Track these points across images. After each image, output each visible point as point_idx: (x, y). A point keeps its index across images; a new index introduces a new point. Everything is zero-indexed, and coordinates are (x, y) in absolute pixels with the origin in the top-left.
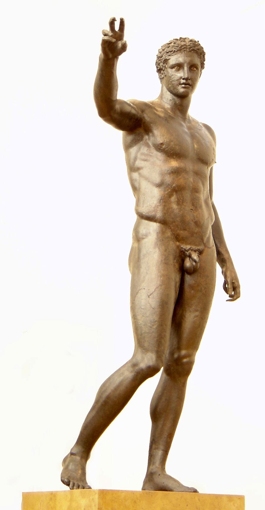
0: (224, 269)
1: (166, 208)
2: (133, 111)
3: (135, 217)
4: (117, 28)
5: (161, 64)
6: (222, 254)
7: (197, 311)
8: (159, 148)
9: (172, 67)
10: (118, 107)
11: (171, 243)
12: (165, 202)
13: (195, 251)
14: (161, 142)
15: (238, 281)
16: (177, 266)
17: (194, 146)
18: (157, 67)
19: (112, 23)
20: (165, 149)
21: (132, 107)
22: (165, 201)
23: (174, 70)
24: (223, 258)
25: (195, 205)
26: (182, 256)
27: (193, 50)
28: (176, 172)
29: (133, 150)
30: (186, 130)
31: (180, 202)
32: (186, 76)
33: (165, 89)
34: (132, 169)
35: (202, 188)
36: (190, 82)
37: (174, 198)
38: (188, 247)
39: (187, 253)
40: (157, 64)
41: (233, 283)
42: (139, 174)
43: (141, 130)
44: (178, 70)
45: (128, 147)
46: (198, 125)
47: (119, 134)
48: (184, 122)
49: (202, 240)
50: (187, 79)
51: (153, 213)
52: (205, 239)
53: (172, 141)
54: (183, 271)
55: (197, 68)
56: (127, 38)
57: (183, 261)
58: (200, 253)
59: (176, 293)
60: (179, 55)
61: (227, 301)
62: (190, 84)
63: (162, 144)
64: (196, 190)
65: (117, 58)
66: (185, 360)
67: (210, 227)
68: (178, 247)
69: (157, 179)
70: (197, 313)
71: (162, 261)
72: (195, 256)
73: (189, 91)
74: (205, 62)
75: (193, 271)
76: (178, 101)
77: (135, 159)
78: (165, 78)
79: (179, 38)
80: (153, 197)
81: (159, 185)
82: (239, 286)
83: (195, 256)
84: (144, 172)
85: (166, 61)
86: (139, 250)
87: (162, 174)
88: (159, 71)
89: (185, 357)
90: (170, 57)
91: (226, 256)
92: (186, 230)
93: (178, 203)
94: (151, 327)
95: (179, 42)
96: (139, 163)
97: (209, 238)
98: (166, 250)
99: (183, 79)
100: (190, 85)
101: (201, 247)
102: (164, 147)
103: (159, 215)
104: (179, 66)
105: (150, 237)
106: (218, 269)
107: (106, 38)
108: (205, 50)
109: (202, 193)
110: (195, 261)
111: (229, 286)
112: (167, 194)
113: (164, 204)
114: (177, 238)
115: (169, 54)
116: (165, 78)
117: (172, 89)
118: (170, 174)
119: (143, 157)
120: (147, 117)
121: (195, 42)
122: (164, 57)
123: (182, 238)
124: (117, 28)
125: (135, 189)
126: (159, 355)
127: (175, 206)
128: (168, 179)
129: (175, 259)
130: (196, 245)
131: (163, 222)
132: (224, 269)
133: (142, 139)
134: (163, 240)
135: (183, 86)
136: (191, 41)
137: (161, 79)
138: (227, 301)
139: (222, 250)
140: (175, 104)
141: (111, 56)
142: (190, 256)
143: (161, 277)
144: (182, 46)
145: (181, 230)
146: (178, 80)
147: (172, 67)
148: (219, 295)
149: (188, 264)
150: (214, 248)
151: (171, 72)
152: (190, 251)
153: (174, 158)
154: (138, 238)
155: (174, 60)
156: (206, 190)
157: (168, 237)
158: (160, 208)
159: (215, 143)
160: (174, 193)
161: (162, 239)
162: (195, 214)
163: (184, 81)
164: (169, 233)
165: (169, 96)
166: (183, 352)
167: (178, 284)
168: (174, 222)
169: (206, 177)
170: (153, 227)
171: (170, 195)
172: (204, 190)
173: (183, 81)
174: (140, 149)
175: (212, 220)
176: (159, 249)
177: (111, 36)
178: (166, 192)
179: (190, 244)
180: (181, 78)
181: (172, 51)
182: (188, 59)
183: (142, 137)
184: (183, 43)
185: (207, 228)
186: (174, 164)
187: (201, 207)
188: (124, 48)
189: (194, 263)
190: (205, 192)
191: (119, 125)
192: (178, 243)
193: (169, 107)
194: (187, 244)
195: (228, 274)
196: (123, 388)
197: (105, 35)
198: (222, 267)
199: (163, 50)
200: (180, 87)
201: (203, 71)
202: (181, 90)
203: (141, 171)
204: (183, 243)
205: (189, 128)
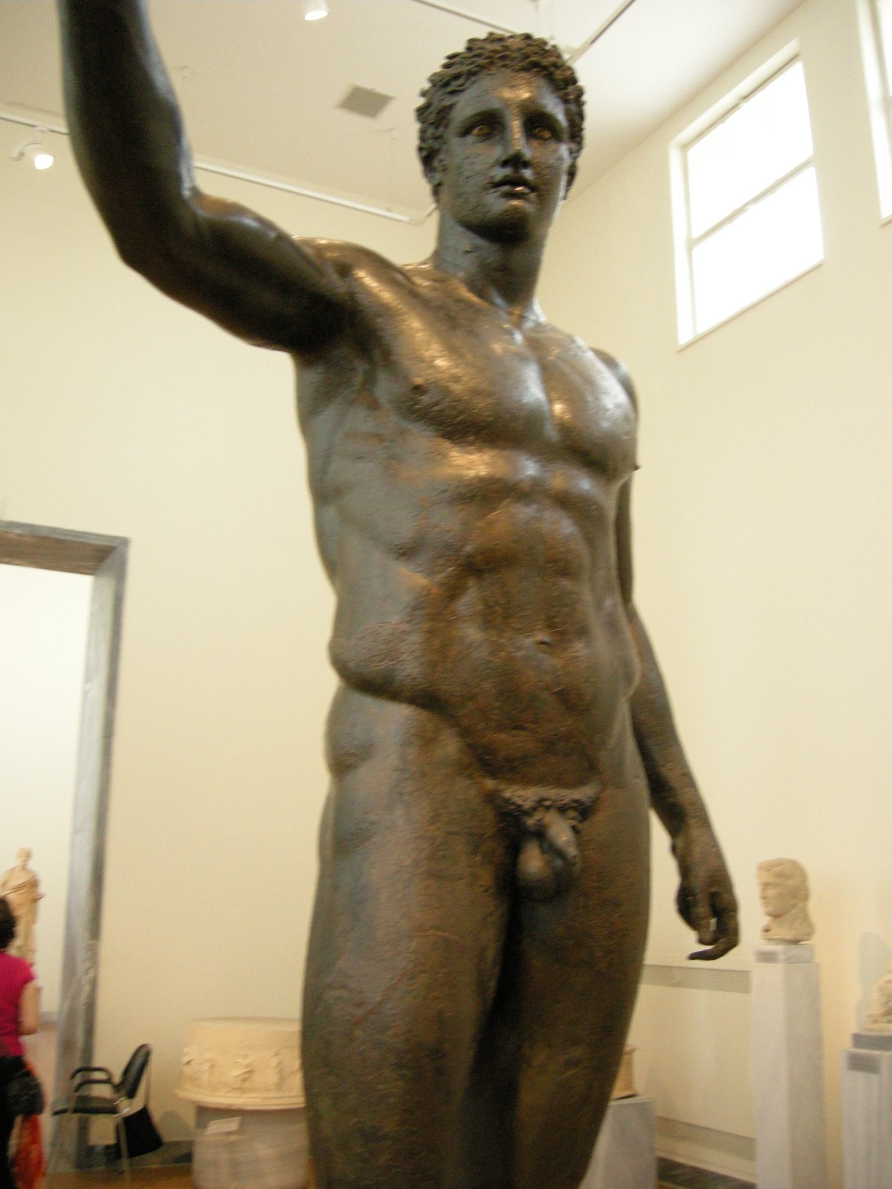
0: (680, 843)
1: (436, 642)
6: (671, 789)
11: (462, 783)
12: (434, 618)
13: (562, 810)
14: (419, 381)
16: (486, 877)
22: (436, 610)
23: (470, 139)
24: (679, 808)
25: (563, 626)
26: (513, 831)
27: (536, 65)
31: (496, 617)
39: (530, 822)
41: (713, 896)
43: (342, 352)
51: (385, 664)
52: (604, 758)
57: (515, 850)
63: (418, 389)
68: (491, 798)
72: (561, 833)
75: (563, 884)
76: (490, 252)
90: (454, 99)
91: (684, 797)
98: (434, 819)
99: (505, 164)
100: (533, 188)
101: (584, 793)
106: (659, 838)
112: (441, 585)
113: (426, 626)
114: (485, 761)
115: (454, 86)
118: (452, 502)
123: (509, 760)
127: (472, 633)
129: (474, 852)
130: (566, 786)
131: (427, 700)
132: (680, 843)
134: (424, 775)
135: (506, 188)
137: (436, 190)
139: (670, 774)
142: (541, 834)
145: (500, 728)
148: (668, 935)
149: (533, 862)
152: (537, 816)
158: (415, 640)
160: (471, 582)
164: (450, 745)
168: (472, 698)
170: (393, 719)
171: (453, 591)
173: (500, 173)
178: (439, 577)
179: (540, 781)
184: (497, 46)
190: (601, 573)
192: (490, 784)
194: (527, 781)
196: (492, 953)
202: (497, 205)
204: (511, 782)
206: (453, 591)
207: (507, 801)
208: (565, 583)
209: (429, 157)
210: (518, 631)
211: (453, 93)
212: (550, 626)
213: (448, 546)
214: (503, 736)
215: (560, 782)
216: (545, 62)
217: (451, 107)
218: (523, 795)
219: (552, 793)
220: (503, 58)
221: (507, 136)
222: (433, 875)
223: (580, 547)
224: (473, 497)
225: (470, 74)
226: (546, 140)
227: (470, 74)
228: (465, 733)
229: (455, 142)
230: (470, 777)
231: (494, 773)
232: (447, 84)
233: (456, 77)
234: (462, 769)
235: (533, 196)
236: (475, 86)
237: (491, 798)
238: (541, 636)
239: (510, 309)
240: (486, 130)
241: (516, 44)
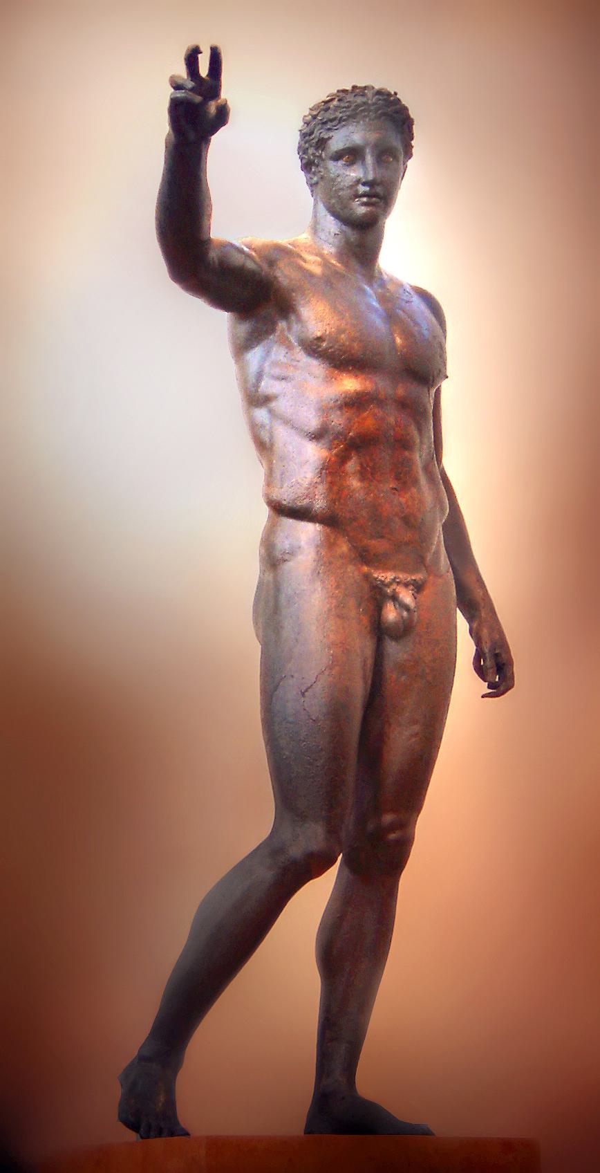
0: (475, 625)
1: (335, 488)
2: (250, 265)
3: (264, 512)
4: (204, 70)
5: (311, 151)
7: (415, 722)
8: (313, 348)
9: (338, 156)
10: (213, 255)
11: (351, 568)
13: (406, 585)
14: (319, 334)
15: (508, 651)
16: (365, 620)
17: (394, 341)
18: (302, 159)
19: (192, 59)
20: (327, 349)
21: (248, 256)
22: (332, 471)
23: (340, 163)
25: (404, 477)
26: (377, 596)
28: (354, 403)
29: (255, 356)
30: (375, 304)
31: (365, 474)
32: (370, 177)
33: (322, 210)
34: (256, 399)
35: (418, 441)
36: (379, 189)
37: (352, 465)
38: (389, 576)
40: (302, 150)
42: (271, 411)
43: (269, 310)
44: (351, 163)
45: (242, 348)
46: (401, 291)
47: (221, 320)
48: (371, 286)
49: (422, 559)
50: (370, 184)
51: (306, 502)
52: (429, 558)
53: (344, 332)
54: (379, 631)
55: (396, 158)
56: (228, 92)
57: (379, 609)
58: (418, 588)
59: (366, 683)
60: (351, 128)
62: (381, 196)
63: (320, 339)
64: (404, 444)
65: (208, 142)
66: (392, 836)
67: (439, 528)
69: (313, 421)
70: (416, 728)
71: (330, 610)
72: (407, 597)
73: (380, 211)
74: (413, 143)
75: (404, 631)
76: (353, 236)
77: (259, 376)
78: (322, 183)
79: (349, 88)
80: (305, 462)
81: (317, 436)
82: (510, 663)
83: (407, 597)
84: (281, 405)
85: (322, 144)
86: (277, 587)
87: (324, 410)
88: (307, 166)
89: (392, 827)
90: (331, 134)
91: (479, 593)
92: (382, 537)
93: (363, 474)
94: (311, 764)
95: (350, 98)
96: (268, 386)
97: (437, 553)
98: (338, 587)
99: (364, 184)
101: (418, 577)
102: (324, 345)
103: (319, 504)
104: (352, 155)
105: (300, 557)
107: (180, 94)
108: (412, 114)
109: (417, 447)
110: (407, 608)
111: (488, 663)
112: (336, 455)
113: (329, 479)
114: (364, 556)
116: (322, 183)
117: (338, 208)
118: (340, 408)
119: (276, 371)
120: (284, 275)
121: (389, 94)
122: (316, 133)
124: (204, 70)
125: (264, 446)
126: (332, 830)
127: (355, 483)
128: (338, 421)
131: (330, 520)
133: (273, 331)
134: (330, 563)
135: (365, 199)
136: (379, 92)
137: (313, 186)
139: (469, 580)
140: (348, 243)
141: (192, 136)
142: (394, 598)
143: (330, 648)
144: (358, 106)
145: (372, 537)
146: (351, 187)
147: (338, 156)
149: (391, 614)
150: (451, 576)
151: (335, 168)
152: (394, 586)
153: (349, 371)
154: (273, 560)
155: (338, 140)
156: (426, 440)
157: (342, 556)
158: (321, 489)
159: (445, 331)
161: (327, 560)
162: (403, 500)
163: (367, 189)
164: (344, 548)
165: (331, 225)
166: (388, 818)
167: (370, 662)
168: (355, 519)
169: (425, 411)
170: (307, 534)
172: (421, 442)
173: (362, 189)
174: (268, 353)
175: (442, 510)
176: (323, 582)
177: (192, 90)
179: (394, 568)
180: (358, 181)
181: (331, 120)
182: (373, 137)
183: (274, 324)
184: (360, 100)
185: (433, 529)
186: (351, 384)
187: (416, 482)
188: (222, 116)
189: (405, 614)
191: (219, 299)
192: (365, 569)
193: (333, 250)
194: (386, 569)
195: (485, 632)
197: (177, 87)
198: (470, 619)
199: (314, 117)
200: (357, 202)
201: (410, 163)
203: (273, 405)
204: (377, 568)
205: (383, 299)
206: (343, 459)
208: (407, 453)
211: (329, 129)
212: (397, 478)
213: (340, 433)
215: (405, 570)
217: (330, 138)
222: (340, 616)
224: (353, 405)
225: (341, 120)
227: (341, 120)
229: (331, 165)
232: (325, 123)
236: (344, 129)
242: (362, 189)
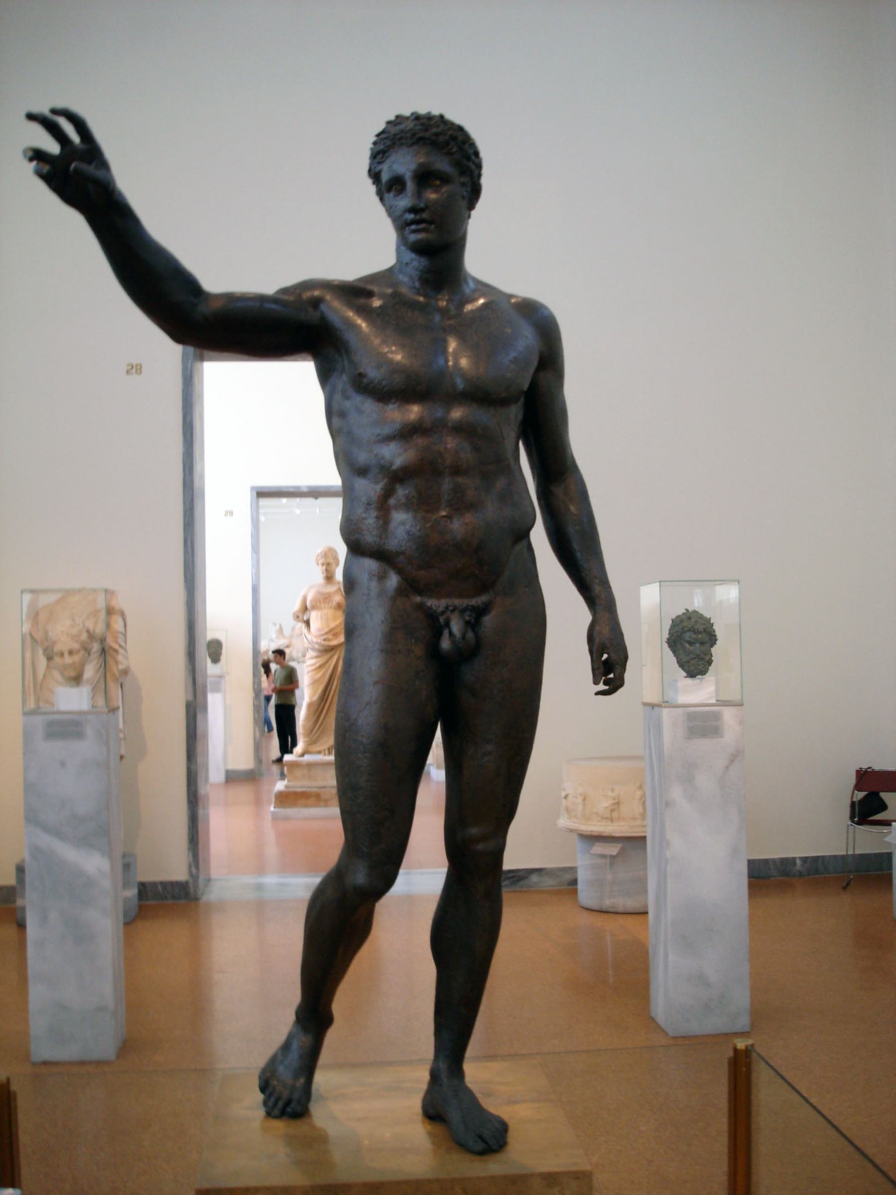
16: (419, 650)
31: (423, 503)
57: (438, 635)
61: (598, 693)
70: (489, 747)
130: (467, 597)
135: (413, 227)
138: (598, 693)
160: (398, 486)
164: (393, 580)
168: (403, 553)
173: (411, 216)
179: (449, 595)
192: (418, 599)
194: (439, 596)
204: (430, 597)
206: (388, 493)
207: (430, 608)
208: (460, 480)
209: (382, 199)
210: (427, 512)
214: (423, 572)
215: (461, 596)
216: (427, 135)
218: (435, 604)
219: (457, 602)
220: (400, 139)
221: (431, 171)
223: (467, 455)
226: (438, 186)
228: (400, 572)
230: (407, 596)
231: (420, 593)
233: (378, 153)
234: (400, 592)
235: (433, 226)
237: (420, 607)
238: (444, 513)
239: (440, 297)
240: (399, 187)
241: (410, 125)
242: (411, 216)
